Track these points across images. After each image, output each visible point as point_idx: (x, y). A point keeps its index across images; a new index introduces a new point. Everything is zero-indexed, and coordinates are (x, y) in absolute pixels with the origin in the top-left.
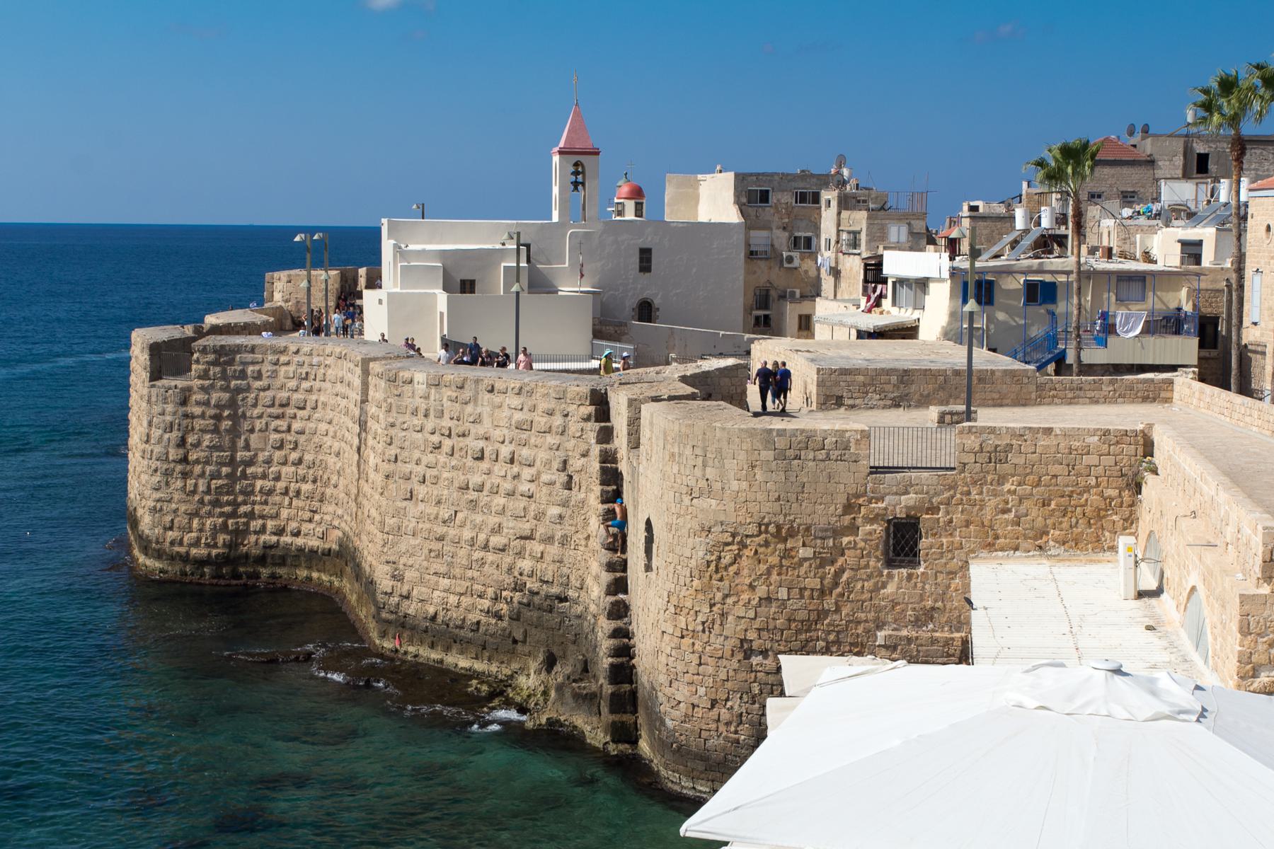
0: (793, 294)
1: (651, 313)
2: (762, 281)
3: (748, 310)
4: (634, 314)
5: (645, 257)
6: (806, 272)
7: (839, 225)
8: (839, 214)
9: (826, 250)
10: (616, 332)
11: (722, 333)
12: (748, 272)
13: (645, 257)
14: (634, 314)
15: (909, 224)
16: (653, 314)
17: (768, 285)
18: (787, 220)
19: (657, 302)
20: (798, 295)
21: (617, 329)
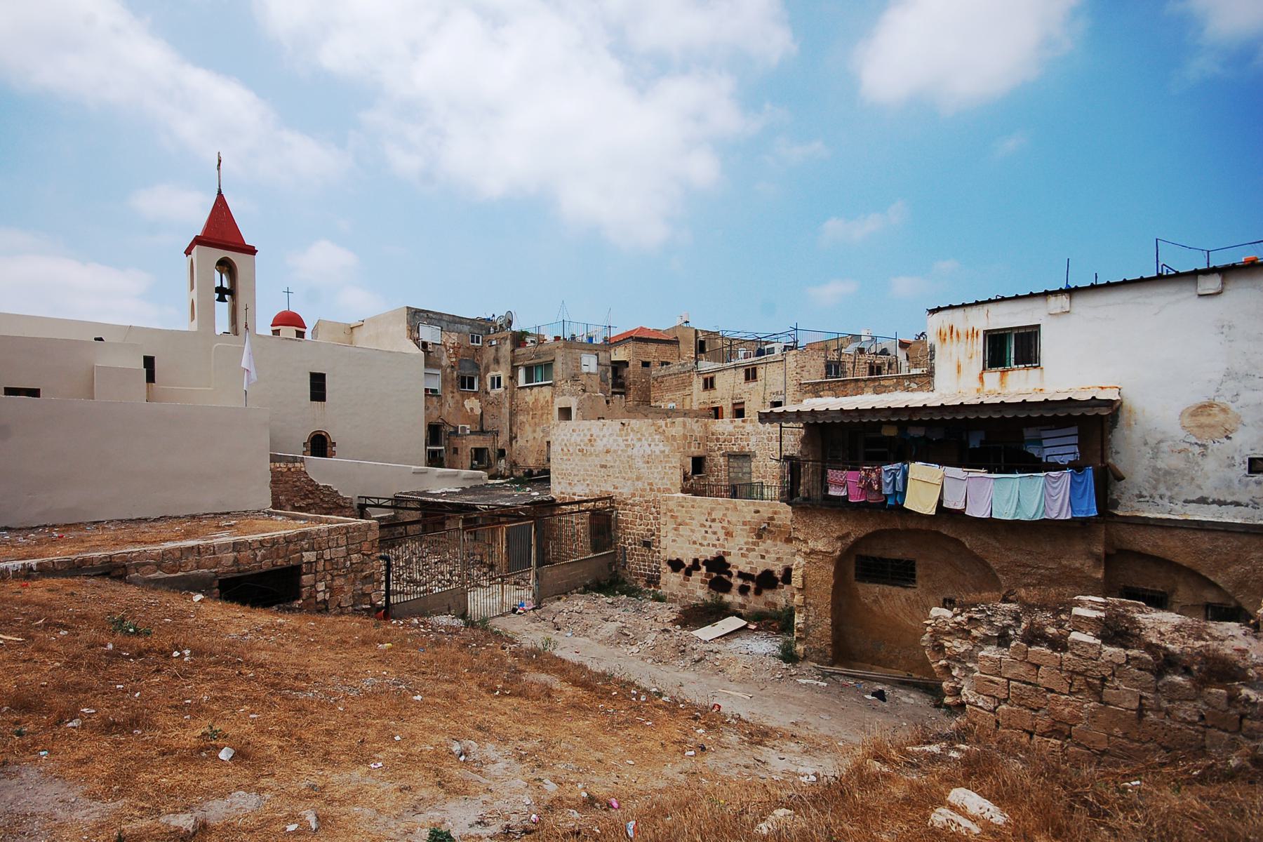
0: (464, 429)
1: (326, 448)
2: (434, 419)
3: (426, 445)
4: (305, 449)
5: (318, 387)
6: (472, 409)
7: (512, 362)
8: (513, 351)
9: (493, 387)
10: (289, 469)
11: (414, 467)
12: (427, 408)
13: (318, 387)
14: (305, 449)
15: (597, 355)
16: (329, 448)
17: (440, 421)
18: (454, 360)
19: (333, 436)
20: (468, 432)
21: (290, 465)
